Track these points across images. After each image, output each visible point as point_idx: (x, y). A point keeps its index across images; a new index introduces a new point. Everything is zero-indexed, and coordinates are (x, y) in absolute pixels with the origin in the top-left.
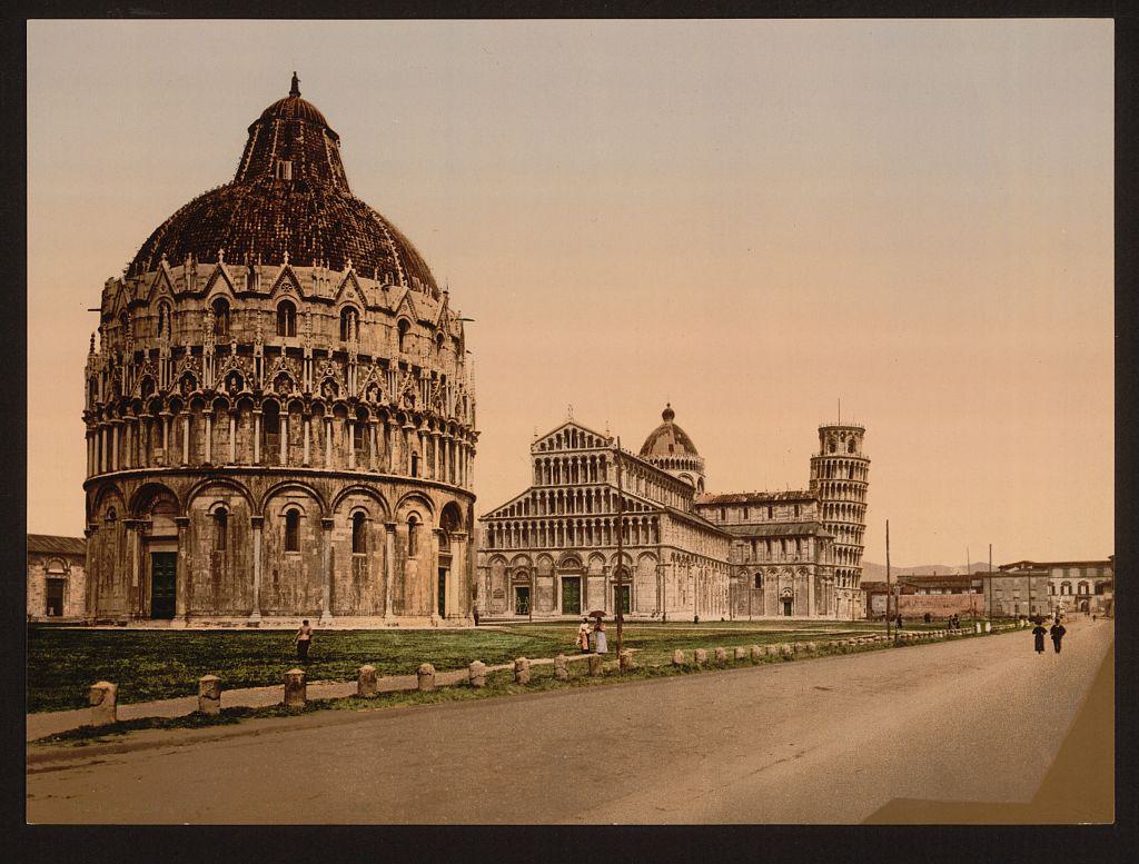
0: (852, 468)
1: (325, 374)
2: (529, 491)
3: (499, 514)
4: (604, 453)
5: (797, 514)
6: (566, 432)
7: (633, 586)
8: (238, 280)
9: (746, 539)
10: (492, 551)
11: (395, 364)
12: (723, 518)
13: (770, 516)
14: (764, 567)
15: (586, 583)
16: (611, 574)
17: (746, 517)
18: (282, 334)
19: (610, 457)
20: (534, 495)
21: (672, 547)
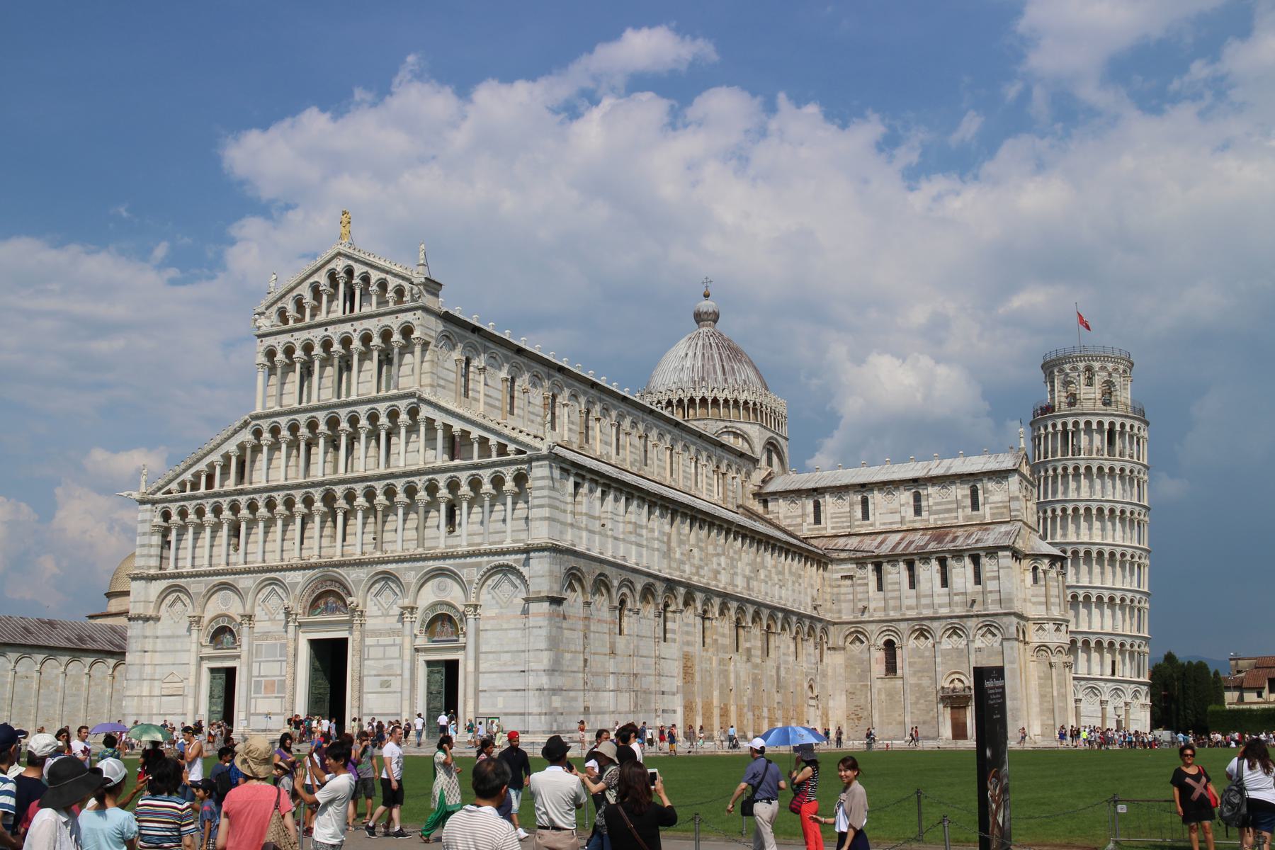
0: (1111, 433)
3: (183, 486)
4: (409, 317)
5: (975, 506)
6: (332, 276)
7: (466, 659)
9: (861, 563)
10: (164, 577)
12: (817, 520)
13: (918, 511)
14: (903, 626)
16: (417, 626)
17: (866, 516)
19: (425, 327)
20: (258, 433)
21: (555, 549)
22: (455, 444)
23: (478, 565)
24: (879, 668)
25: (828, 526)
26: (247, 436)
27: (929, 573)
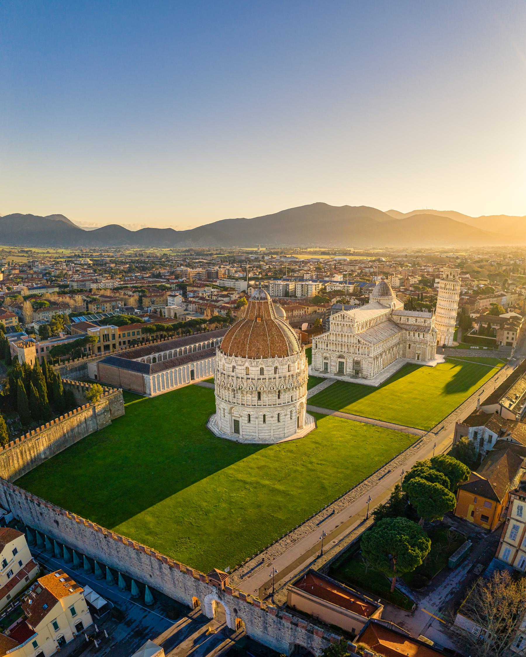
18: (261, 374)
24: (407, 348)
25: (402, 322)
27: (417, 335)
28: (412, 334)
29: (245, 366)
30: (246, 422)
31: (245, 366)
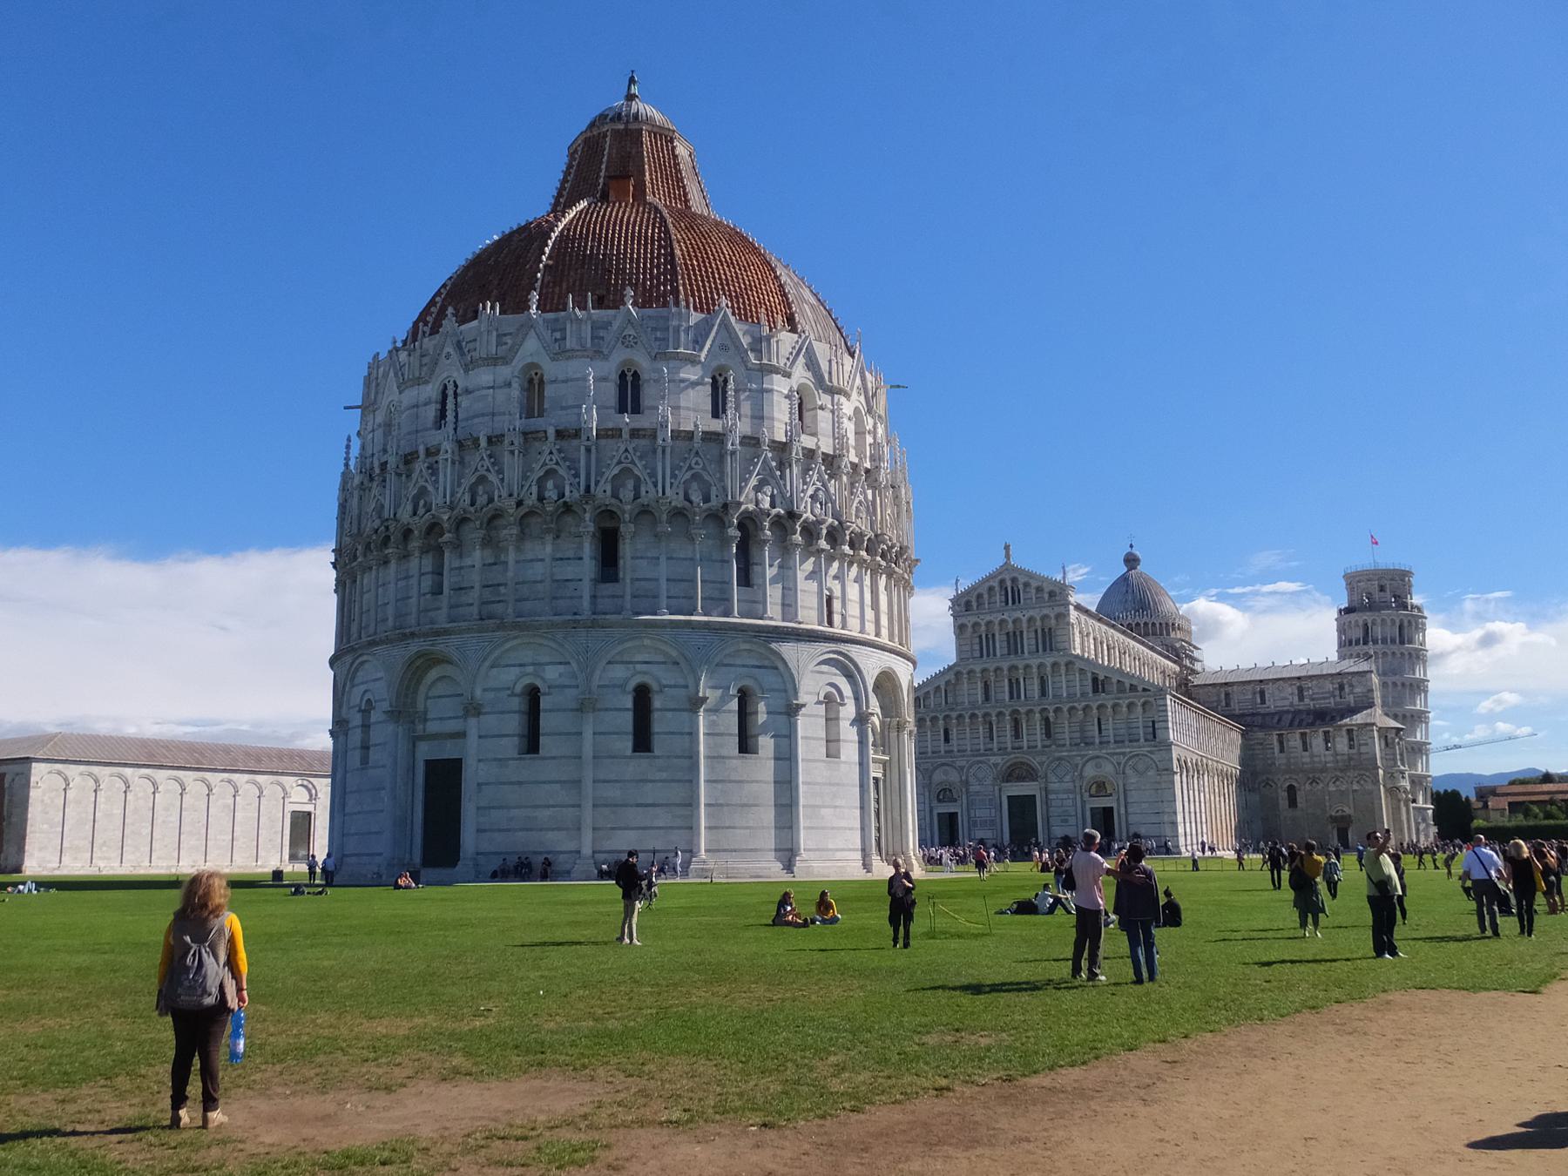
0: (1401, 627)
1: (690, 468)
2: (950, 668)
4: (1062, 609)
8: (558, 335)
11: (796, 453)
13: (1301, 698)
15: (1047, 802)
20: (958, 674)
22: (1098, 685)
23: (1124, 754)
24: (1283, 803)
26: (951, 676)
27: (1317, 742)
28: (1294, 740)
29: (519, 363)
30: (510, 746)
31: (519, 363)
